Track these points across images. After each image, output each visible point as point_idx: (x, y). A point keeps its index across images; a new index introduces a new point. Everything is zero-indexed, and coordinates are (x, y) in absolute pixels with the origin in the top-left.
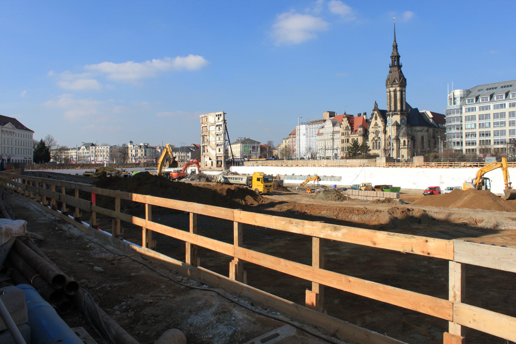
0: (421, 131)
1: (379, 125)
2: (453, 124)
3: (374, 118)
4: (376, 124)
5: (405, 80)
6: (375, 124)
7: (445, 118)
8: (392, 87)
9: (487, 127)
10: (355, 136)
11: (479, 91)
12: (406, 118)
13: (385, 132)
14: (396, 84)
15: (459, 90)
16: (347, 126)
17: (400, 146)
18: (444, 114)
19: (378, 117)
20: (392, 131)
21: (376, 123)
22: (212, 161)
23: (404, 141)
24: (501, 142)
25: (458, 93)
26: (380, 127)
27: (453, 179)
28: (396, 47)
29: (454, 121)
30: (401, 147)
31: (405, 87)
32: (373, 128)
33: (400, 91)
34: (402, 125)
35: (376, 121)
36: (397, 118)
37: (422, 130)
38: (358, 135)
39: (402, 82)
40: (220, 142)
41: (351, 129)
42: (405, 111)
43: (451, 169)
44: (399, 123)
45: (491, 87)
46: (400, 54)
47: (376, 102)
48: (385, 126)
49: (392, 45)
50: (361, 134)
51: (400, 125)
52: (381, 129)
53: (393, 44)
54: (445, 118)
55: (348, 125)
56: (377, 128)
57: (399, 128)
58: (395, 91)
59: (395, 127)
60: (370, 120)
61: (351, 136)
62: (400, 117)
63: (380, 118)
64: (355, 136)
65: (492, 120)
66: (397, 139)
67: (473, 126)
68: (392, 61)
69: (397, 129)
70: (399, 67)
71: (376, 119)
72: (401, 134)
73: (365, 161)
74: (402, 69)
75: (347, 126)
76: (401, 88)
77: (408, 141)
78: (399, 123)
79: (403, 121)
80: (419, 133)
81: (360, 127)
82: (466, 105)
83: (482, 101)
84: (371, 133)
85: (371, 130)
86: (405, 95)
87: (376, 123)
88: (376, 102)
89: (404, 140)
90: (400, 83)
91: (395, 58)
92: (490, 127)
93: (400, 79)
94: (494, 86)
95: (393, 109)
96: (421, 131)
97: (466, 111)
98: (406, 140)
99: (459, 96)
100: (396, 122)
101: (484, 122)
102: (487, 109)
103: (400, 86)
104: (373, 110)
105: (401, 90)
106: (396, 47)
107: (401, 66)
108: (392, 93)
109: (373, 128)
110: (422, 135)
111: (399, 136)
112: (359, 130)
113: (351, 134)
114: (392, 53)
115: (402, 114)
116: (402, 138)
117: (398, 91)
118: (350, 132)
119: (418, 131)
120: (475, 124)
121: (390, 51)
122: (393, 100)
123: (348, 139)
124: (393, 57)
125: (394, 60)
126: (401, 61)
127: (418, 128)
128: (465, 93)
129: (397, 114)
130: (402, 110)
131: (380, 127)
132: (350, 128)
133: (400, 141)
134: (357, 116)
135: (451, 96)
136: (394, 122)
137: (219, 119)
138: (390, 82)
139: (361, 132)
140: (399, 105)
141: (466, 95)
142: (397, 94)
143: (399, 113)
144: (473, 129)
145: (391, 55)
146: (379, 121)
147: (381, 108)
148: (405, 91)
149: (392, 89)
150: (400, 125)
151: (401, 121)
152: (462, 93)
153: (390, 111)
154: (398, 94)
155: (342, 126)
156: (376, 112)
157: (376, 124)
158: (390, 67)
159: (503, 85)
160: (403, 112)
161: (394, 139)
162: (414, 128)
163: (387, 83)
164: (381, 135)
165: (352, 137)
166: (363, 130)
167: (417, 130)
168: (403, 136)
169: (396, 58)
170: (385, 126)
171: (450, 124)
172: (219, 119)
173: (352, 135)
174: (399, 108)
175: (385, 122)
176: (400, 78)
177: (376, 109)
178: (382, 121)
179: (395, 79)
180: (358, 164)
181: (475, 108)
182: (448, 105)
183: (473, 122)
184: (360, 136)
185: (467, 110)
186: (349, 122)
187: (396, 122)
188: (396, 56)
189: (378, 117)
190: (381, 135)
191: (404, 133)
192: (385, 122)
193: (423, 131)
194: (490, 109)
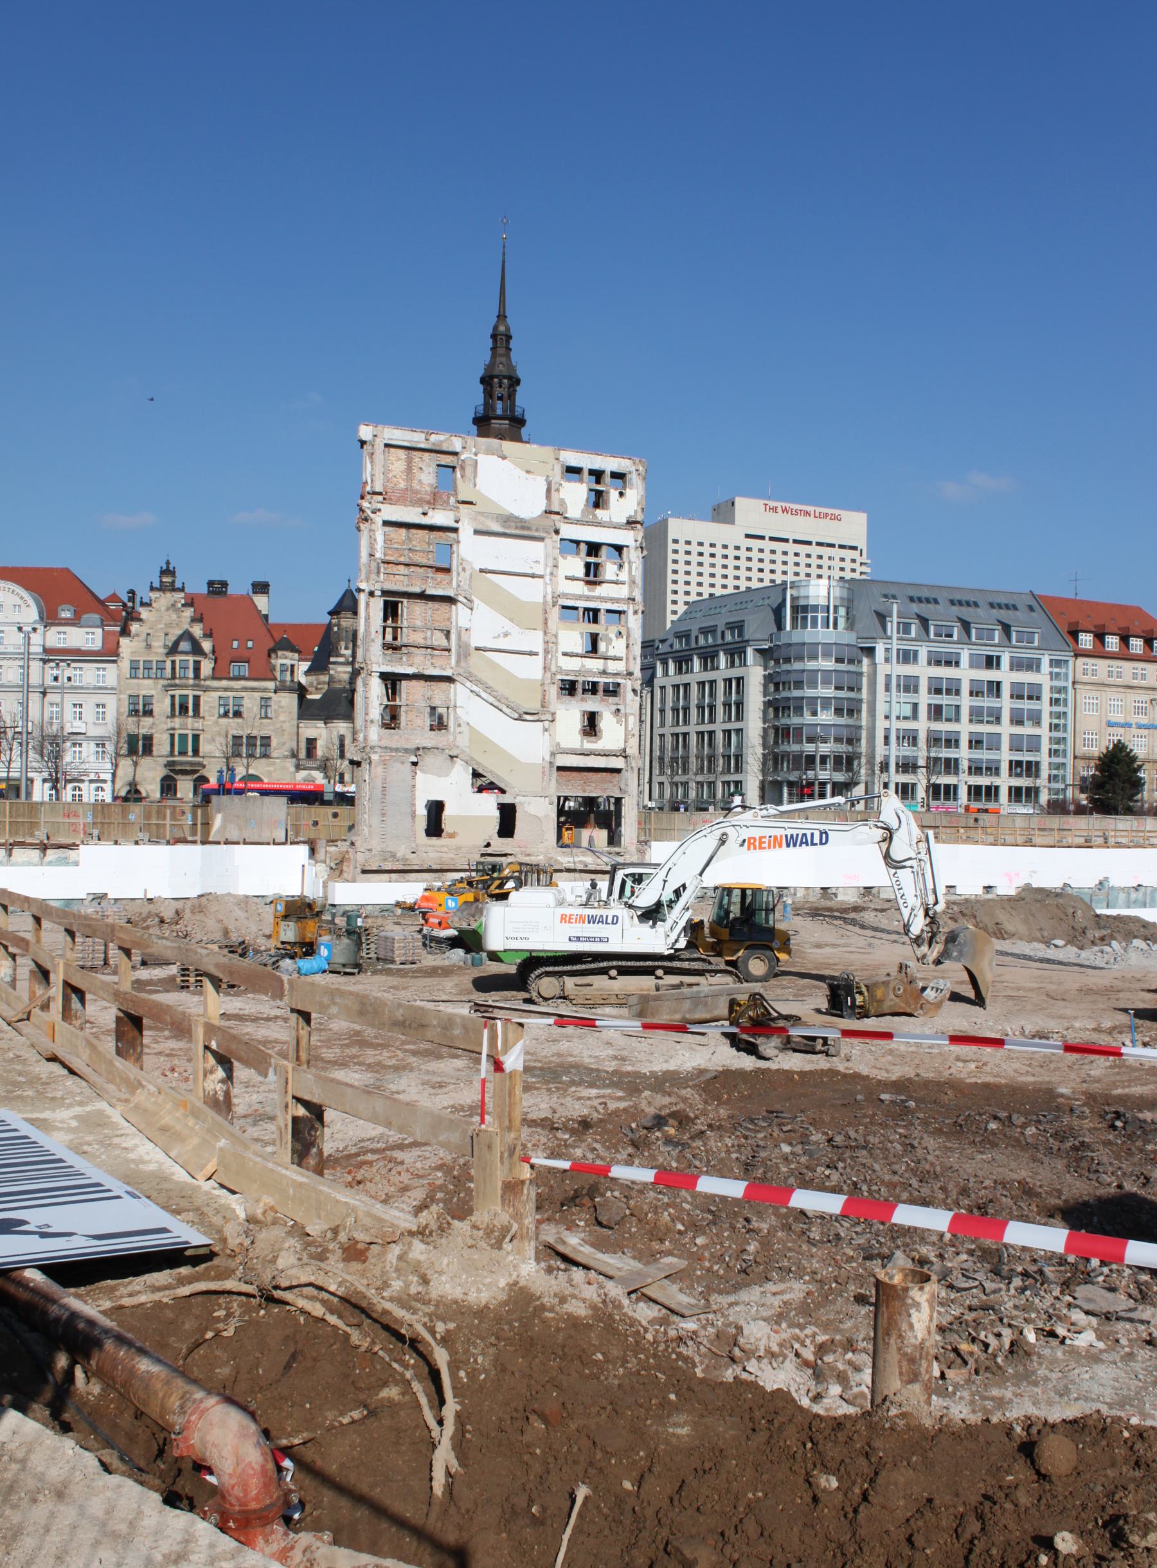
22: (506, 799)
24: (987, 769)
28: (501, 340)
38: (271, 685)
40: (594, 664)
53: (496, 328)
65: (966, 701)
67: (907, 710)
83: (936, 635)
101: (944, 703)
102: (948, 663)
106: (501, 340)
120: (958, 707)
121: (481, 356)
137: (598, 500)
144: (905, 718)
155: (134, 627)
159: (958, 597)
171: (797, 693)
172: (598, 500)
173: (215, 684)
181: (916, 653)
182: (788, 628)
183: (911, 698)
194: (998, 666)
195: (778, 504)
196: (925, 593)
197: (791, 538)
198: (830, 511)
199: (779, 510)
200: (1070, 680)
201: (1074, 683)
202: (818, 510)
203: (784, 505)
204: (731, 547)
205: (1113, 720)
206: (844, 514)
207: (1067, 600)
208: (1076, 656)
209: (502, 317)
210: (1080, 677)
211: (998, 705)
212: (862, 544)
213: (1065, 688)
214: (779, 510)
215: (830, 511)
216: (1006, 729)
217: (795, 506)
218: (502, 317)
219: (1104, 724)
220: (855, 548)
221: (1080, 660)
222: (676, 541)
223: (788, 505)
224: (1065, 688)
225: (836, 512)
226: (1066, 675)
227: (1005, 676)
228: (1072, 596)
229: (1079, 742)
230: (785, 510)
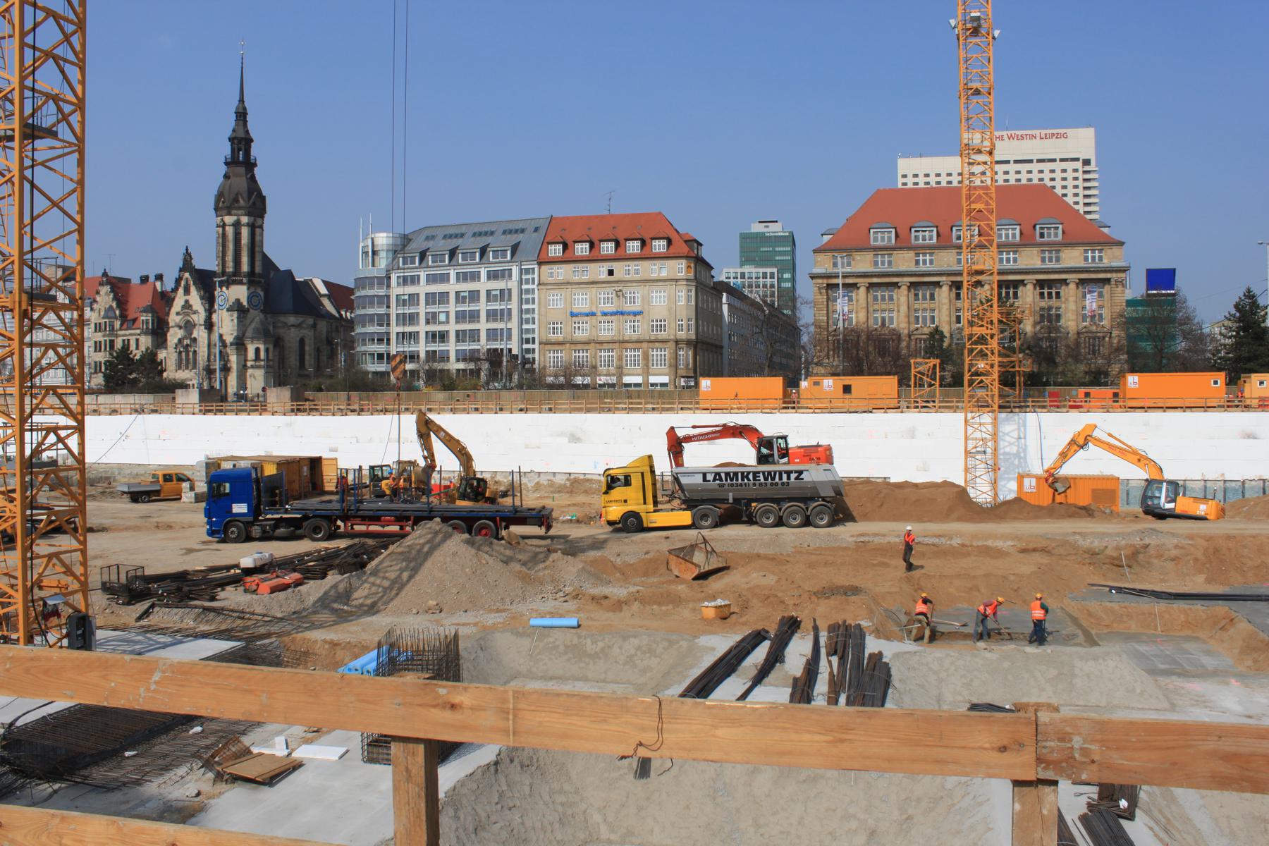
0: (298, 326)
1: (195, 308)
2: (370, 311)
3: (181, 291)
4: (187, 306)
5: (263, 199)
6: (183, 303)
7: (352, 297)
8: (229, 214)
9: (443, 323)
10: (131, 335)
11: (427, 238)
12: (262, 294)
13: (209, 325)
14: (239, 208)
15: (385, 235)
16: (111, 306)
17: (246, 360)
18: (352, 286)
19: (193, 289)
20: (227, 325)
21: (187, 301)
23: (257, 350)
25: (383, 239)
26: (195, 312)
27: (357, 442)
28: (242, 115)
29: (372, 304)
30: (249, 364)
31: (262, 217)
32: (178, 314)
33: (248, 225)
34: (251, 310)
35: (187, 297)
36: (239, 292)
37: (302, 322)
38: (138, 331)
39: (254, 203)
41: (121, 316)
42: (260, 276)
43: (353, 419)
44: (245, 303)
45: (452, 231)
46: (253, 134)
47: (187, 250)
48: (210, 311)
49: (234, 110)
50: (147, 328)
51: (248, 310)
52: (200, 317)
53: (237, 108)
54: (352, 297)
55: (114, 305)
56: (188, 315)
57: (244, 317)
58: (237, 225)
59: (235, 314)
60: (173, 295)
61: (120, 333)
62: (248, 289)
63: (198, 289)
64: (131, 335)
65: (452, 307)
66: (240, 344)
68: (233, 150)
69: (240, 319)
70: (250, 165)
71: (187, 291)
72: (249, 333)
73: (146, 399)
74: (256, 171)
75: (111, 306)
76: (252, 218)
77: (267, 350)
78: (245, 303)
79: (255, 300)
80: (293, 330)
81: (144, 311)
82: (399, 268)
84: (172, 327)
85: (174, 319)
86: (262, 235)
87: (187, 301)
88: (187, 250)
89: (257, 346)
90: (250, 207)
91: (240, 143)
92: (447, 322)
93: (249, 199)
94: (458, 231)
95: (230, 268)
96: (298, 326)
97: (399, 284)
98: (262, 347)
99: (385, 248)
100: (238, 301)
103: (248, 214)
104: (181, 270)
105: (250, 223)
106: (242, 115)
107: (255, 165)
108: (230, 231)
109: (178, 314)
110: (301, 335)
111: (244, 335)
112: (142, 318)
113: (121, 329)
114: (234, 131)
115: (251, 284)
116: (252, 343)
117: (244, 225)
118: (117, 324)
119: (293, 326)
121: (228, 124)
122: (231, 246)
123: (112, 342)
124: (236, 141)
125: (236, 147)
126: (255, 151)
127: (292, 320)
128: (399, 242)
129: (241, 283)
130: (252, 273)
131: (195, 312)
132: (118, 312)
133: (246, 350)
134: (139, 282)
135: (368, 246)
136: (232, 300)
138: (224, 203)
139: (147, 323)
140: (245, 259)
141: (400, 247)
142: (241, 233)
143: (245, 280)
145: (229, 133)
146: (195, 299)
147: (199, 263)
148: (261, 227)
149: (229, 219)
150: (248, 310)
151: (249, 299)
152: (390, 241)
153: (224, 273)
154: (245, 232)
155: (95, 306)
156: (187, 275)
157: (187, 306)
158: (226, 164)
160: (258, 279)
161: (231, 344)
162: (282, 319)
163: (217, 203)
164: (200, 334)
165: (124, 335)
166: (153, 320)
167: (289, 324)
168: (253, 339)
169: (241, 143)
170: (210, 311)
174: (245, 268)
175: (209, 300)
176: (250, 193)
177: (187, 265)
178: (202, 298)
179: (237, 195)
180: (129, 406)
181: (419, 276)
184: (145, 333)
185: (401, 280)
186: (116, 298)
187: (238, 301)
188: (242, 138)
189: (193, 289)
190: (200, 334)
191: (257, 330)
192: (209, 300)
193: (304, 325)
194: (448, 280)
195: (1004, 133)
196: (486, 229)
197: (1012, 159)
198: (1055, 131)
199: (1005, 137)
200: (536, 282)
201: (539, 284)
202: (1043, 132)
203: (1009, 133)
204: (932, 175)
205: (606, 310)
206: (1070, 132)
207: (603, 217)
208: (540, 264)
209: (242, 100)
210: (543, 280)
211: (477, 308)
212: (1091, 155)
213: (533, 290)
214: (1005, 137)
215: (1055, 131)
216: (483, 326)
217: (1020, 133)
218: (242, 100)
219: (568, 314)
220: (1077, 160)
221: (544, 268)
222: (904, 176)
223: (1013, 133)
224: (533, 290)
225: (1062, 131)
226: (533, 279)
227: (483, 285)
228: (606, 213)
229: (543, 330)
230: (1010, 137)
